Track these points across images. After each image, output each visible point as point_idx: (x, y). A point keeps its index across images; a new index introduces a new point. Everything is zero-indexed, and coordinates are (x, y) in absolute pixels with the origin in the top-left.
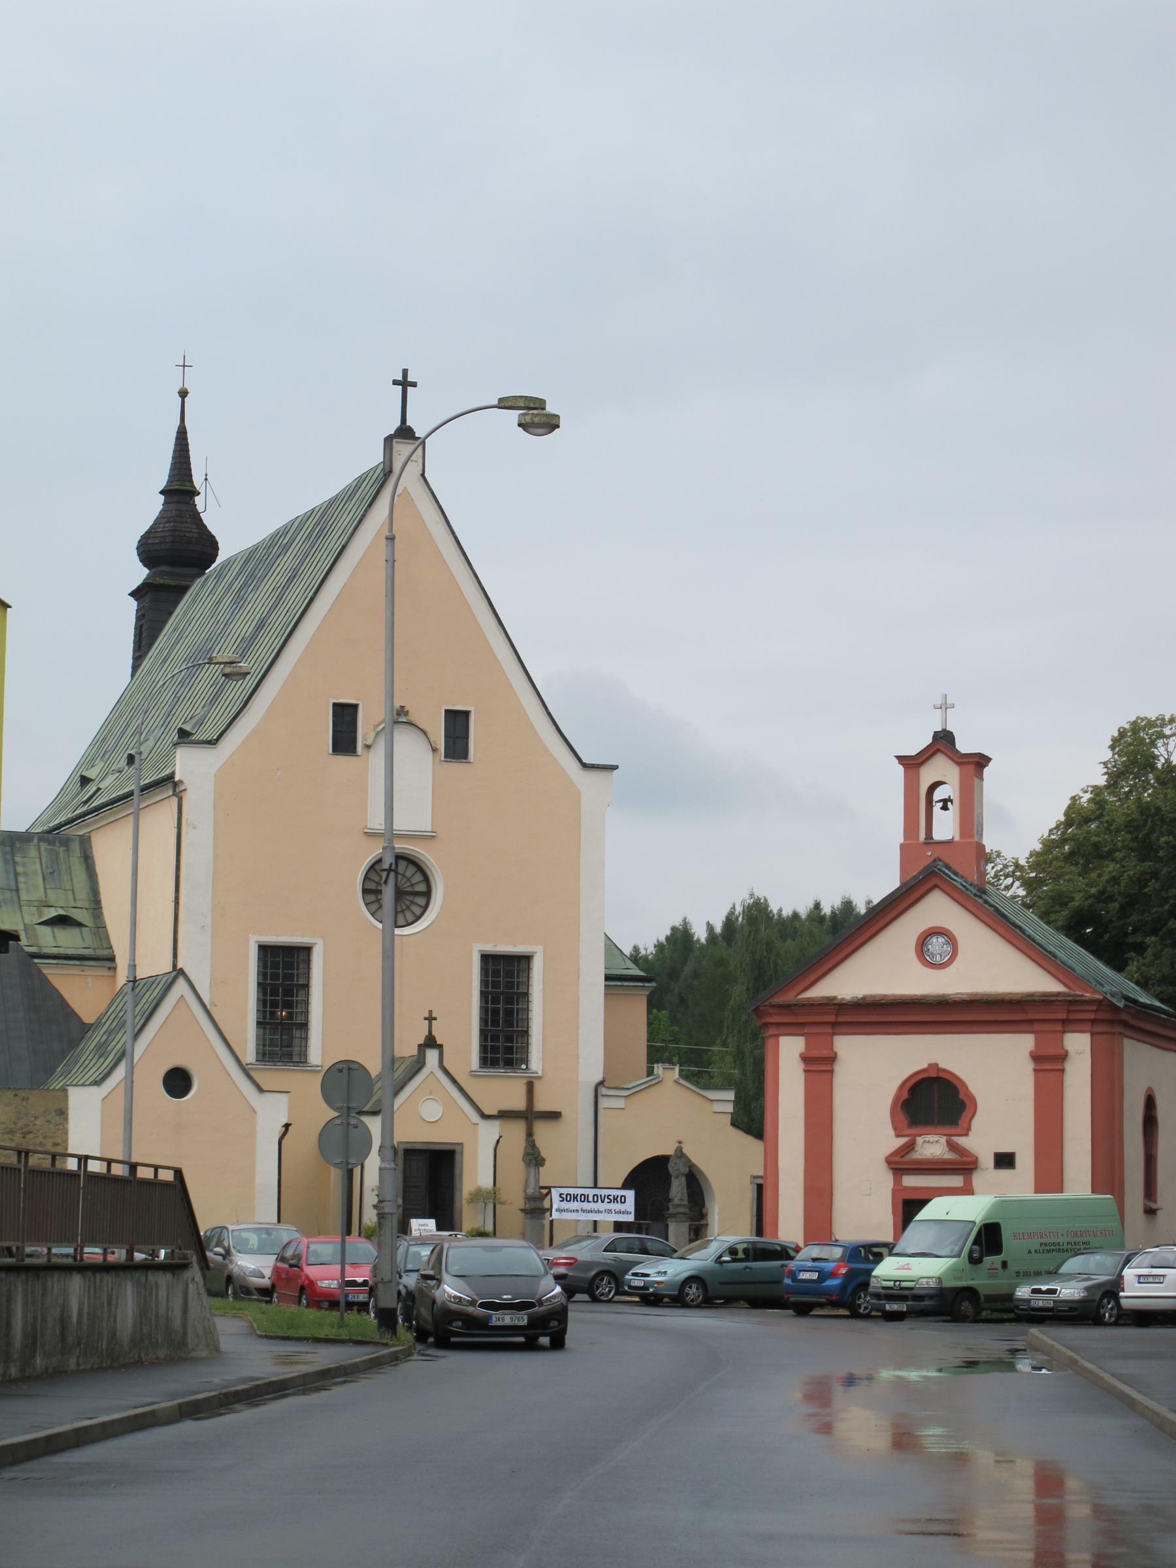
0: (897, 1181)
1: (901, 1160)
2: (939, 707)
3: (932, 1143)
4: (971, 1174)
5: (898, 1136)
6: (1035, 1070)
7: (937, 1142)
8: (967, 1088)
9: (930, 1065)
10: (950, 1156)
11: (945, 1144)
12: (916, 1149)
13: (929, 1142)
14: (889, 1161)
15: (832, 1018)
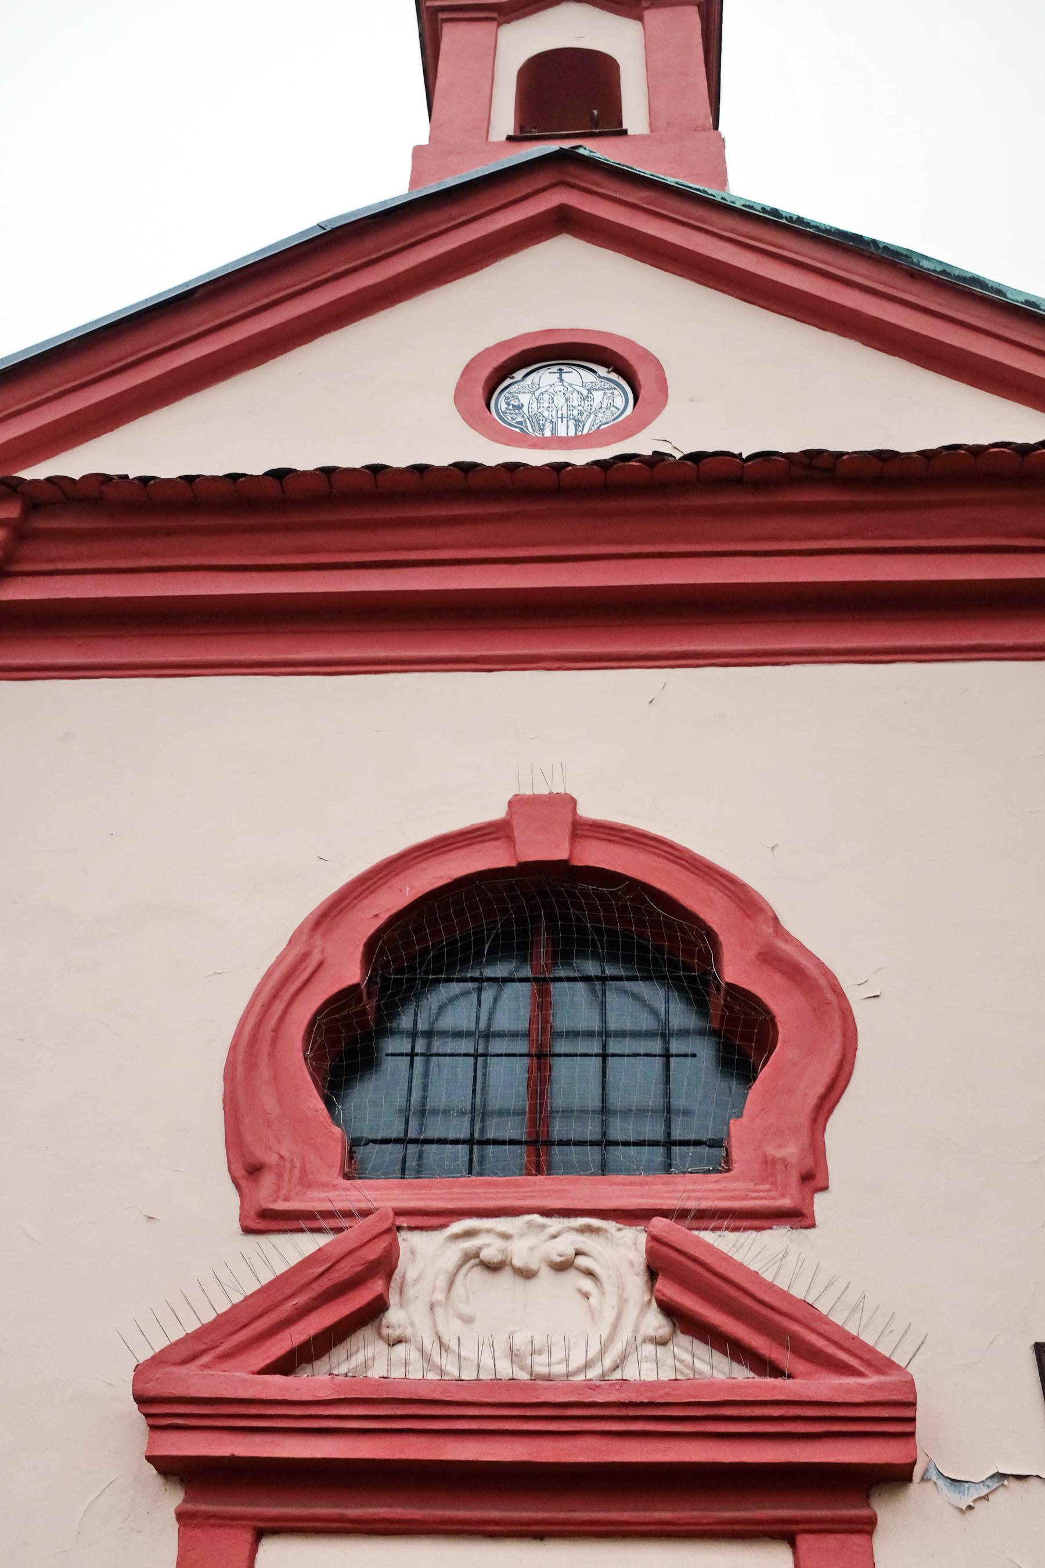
1: (277, 1386)
3: (526, 1274)
4: (867, 1526)
7: (561, 1267)
8: (776, 919)
9: (517, 803)
11: (636, 1285)
12: (394, 1315)
13: (493, 1267)
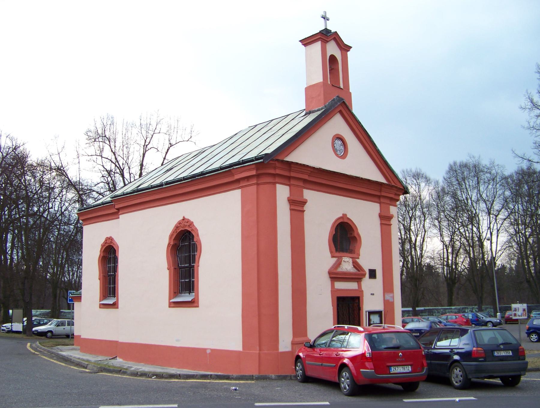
0: (333, 286)
2: (324, 17)
3: (346, 262)
4: (361, 281)
5: (333, 257)
6: (381, 224)
10: (353, 270)
14: (330, 273)
15: (306, 177)
